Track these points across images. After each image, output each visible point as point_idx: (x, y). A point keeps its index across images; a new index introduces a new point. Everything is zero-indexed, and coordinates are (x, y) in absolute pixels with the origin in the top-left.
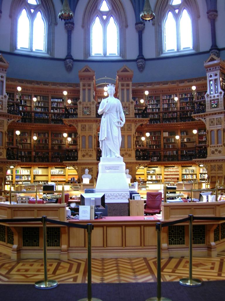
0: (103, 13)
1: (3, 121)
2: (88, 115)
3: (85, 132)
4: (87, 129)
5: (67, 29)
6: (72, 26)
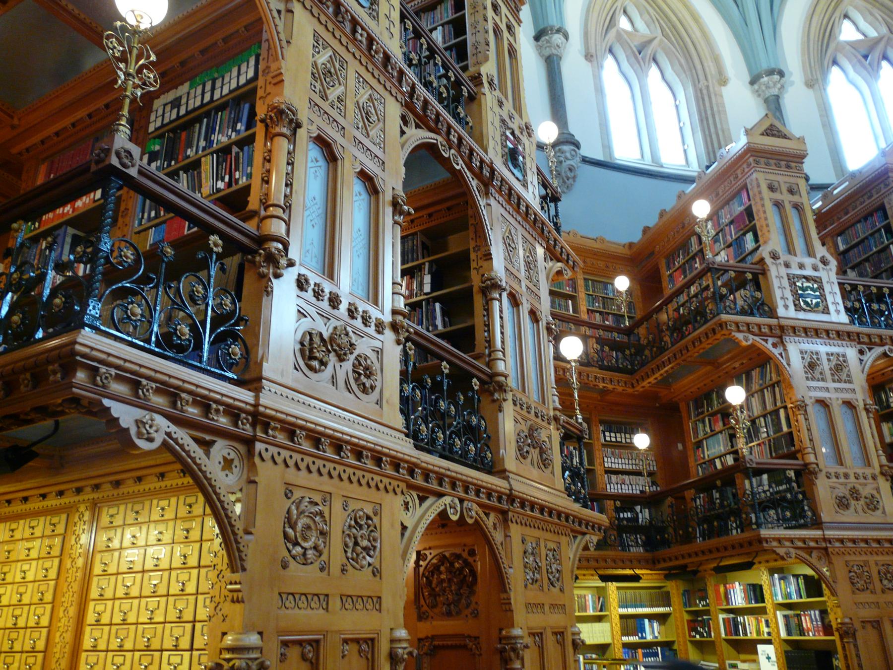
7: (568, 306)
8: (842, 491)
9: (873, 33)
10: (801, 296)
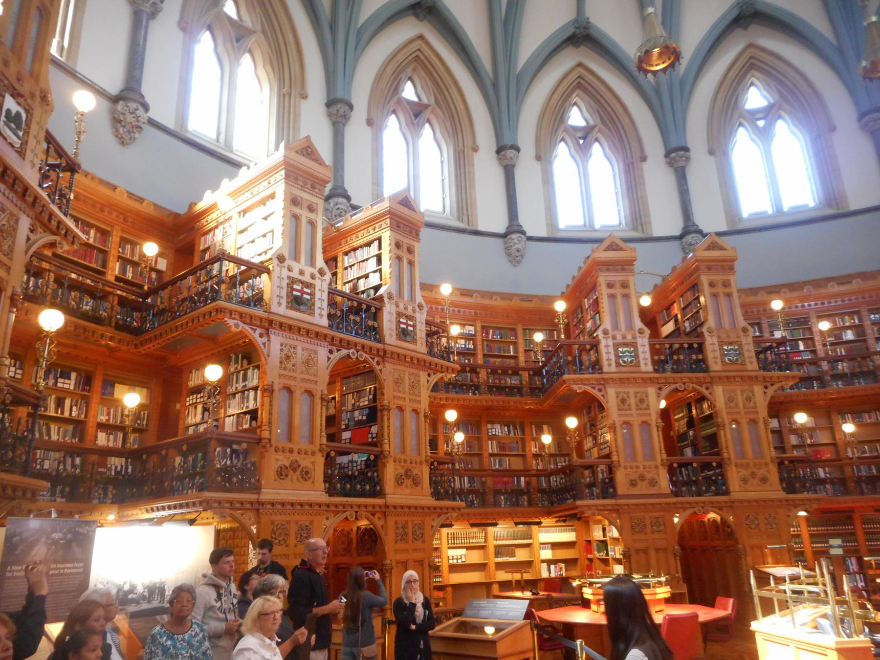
8: (634, 477)
10: (621, 357)
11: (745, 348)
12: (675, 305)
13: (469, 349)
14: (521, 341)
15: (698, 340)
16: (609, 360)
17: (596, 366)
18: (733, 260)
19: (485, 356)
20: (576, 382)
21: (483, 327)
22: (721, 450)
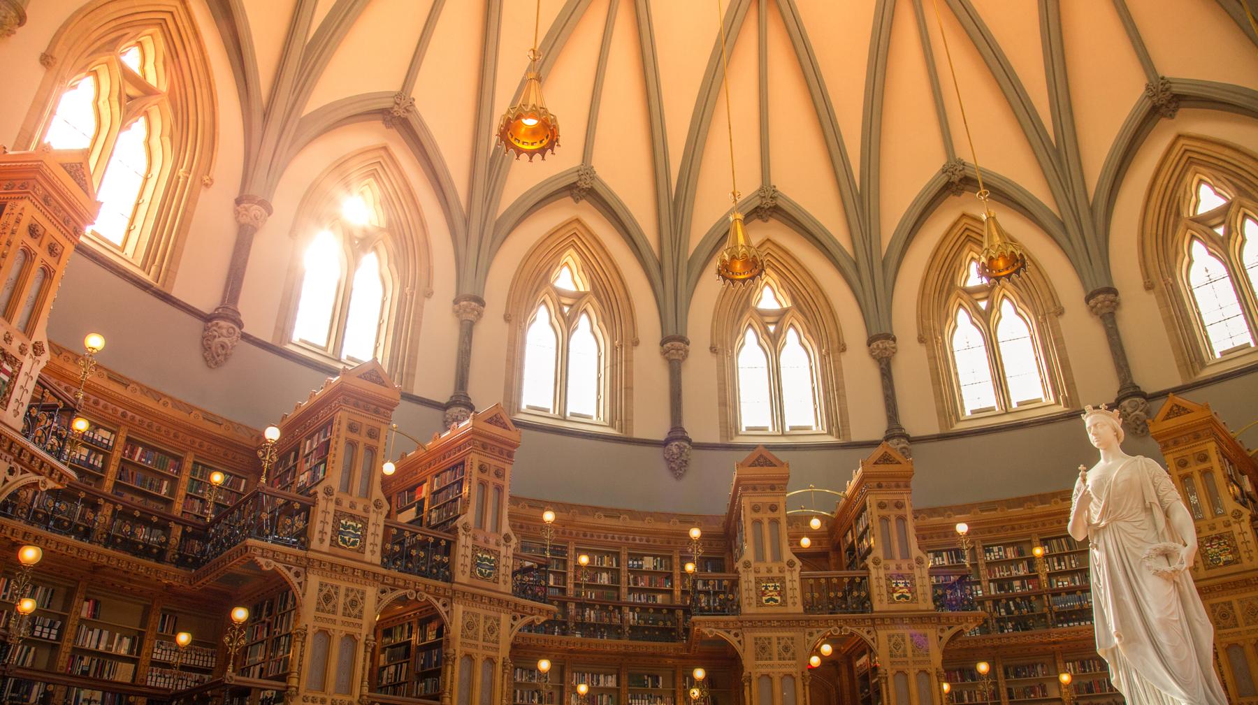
0: (1205, 222)
1: (925, 636)
2: (1227, 563)
3: (1236, 629)
4: (1240, 620)
5: (1096, 314)
6: (1111, 297)
7: (160, 487)
9: (582, 289)
10: (341, 533)
11: (503, 561)
12: (425, 487)
13: (92, 467)
14: (185, 478)
15: (450, 537)
16: (322, 532)
17: (302, 539)
18: (515, 446)
19: (117, 485)
20: (266, 553)
21: (128, 439)
22: (443, 692)
